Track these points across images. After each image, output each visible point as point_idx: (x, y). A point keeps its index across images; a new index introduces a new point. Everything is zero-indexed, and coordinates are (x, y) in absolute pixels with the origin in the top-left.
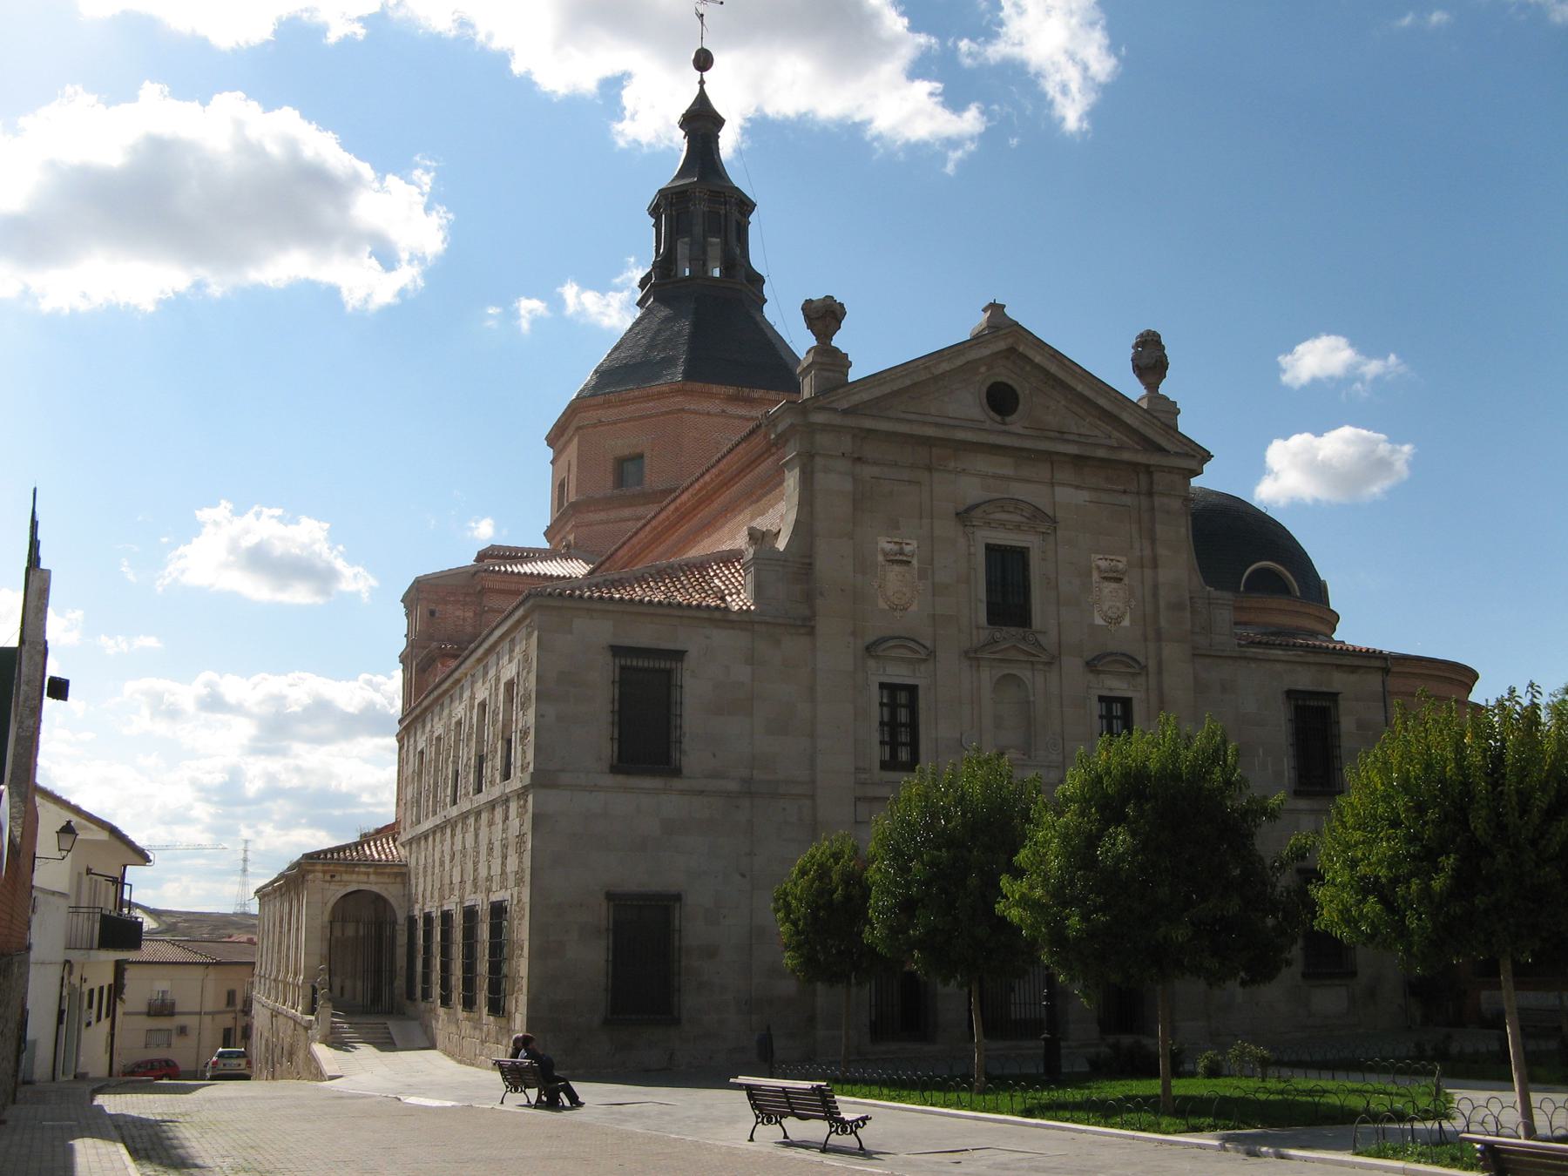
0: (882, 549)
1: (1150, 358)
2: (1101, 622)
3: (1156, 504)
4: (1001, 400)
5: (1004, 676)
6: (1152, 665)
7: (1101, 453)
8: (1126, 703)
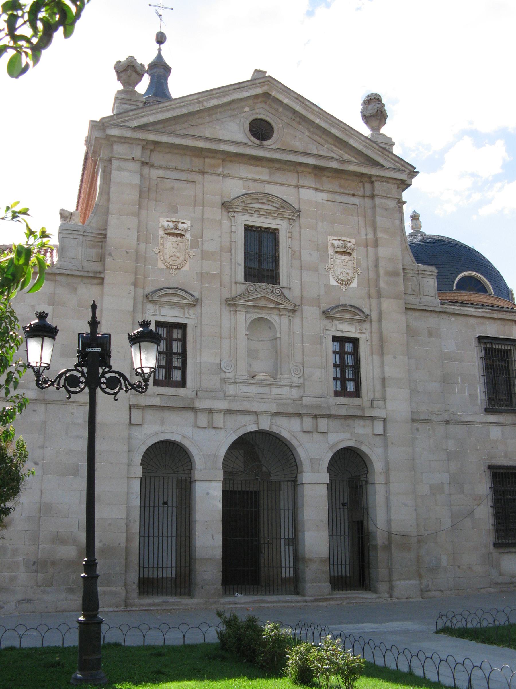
0: (163, 226)
1: (375, 111)
2: (336, 284)
3: (377, 203)
4: (261, 130)
5: (259, 319)
6: (374, 316)
7: (334, 165)
8: (355, 341)
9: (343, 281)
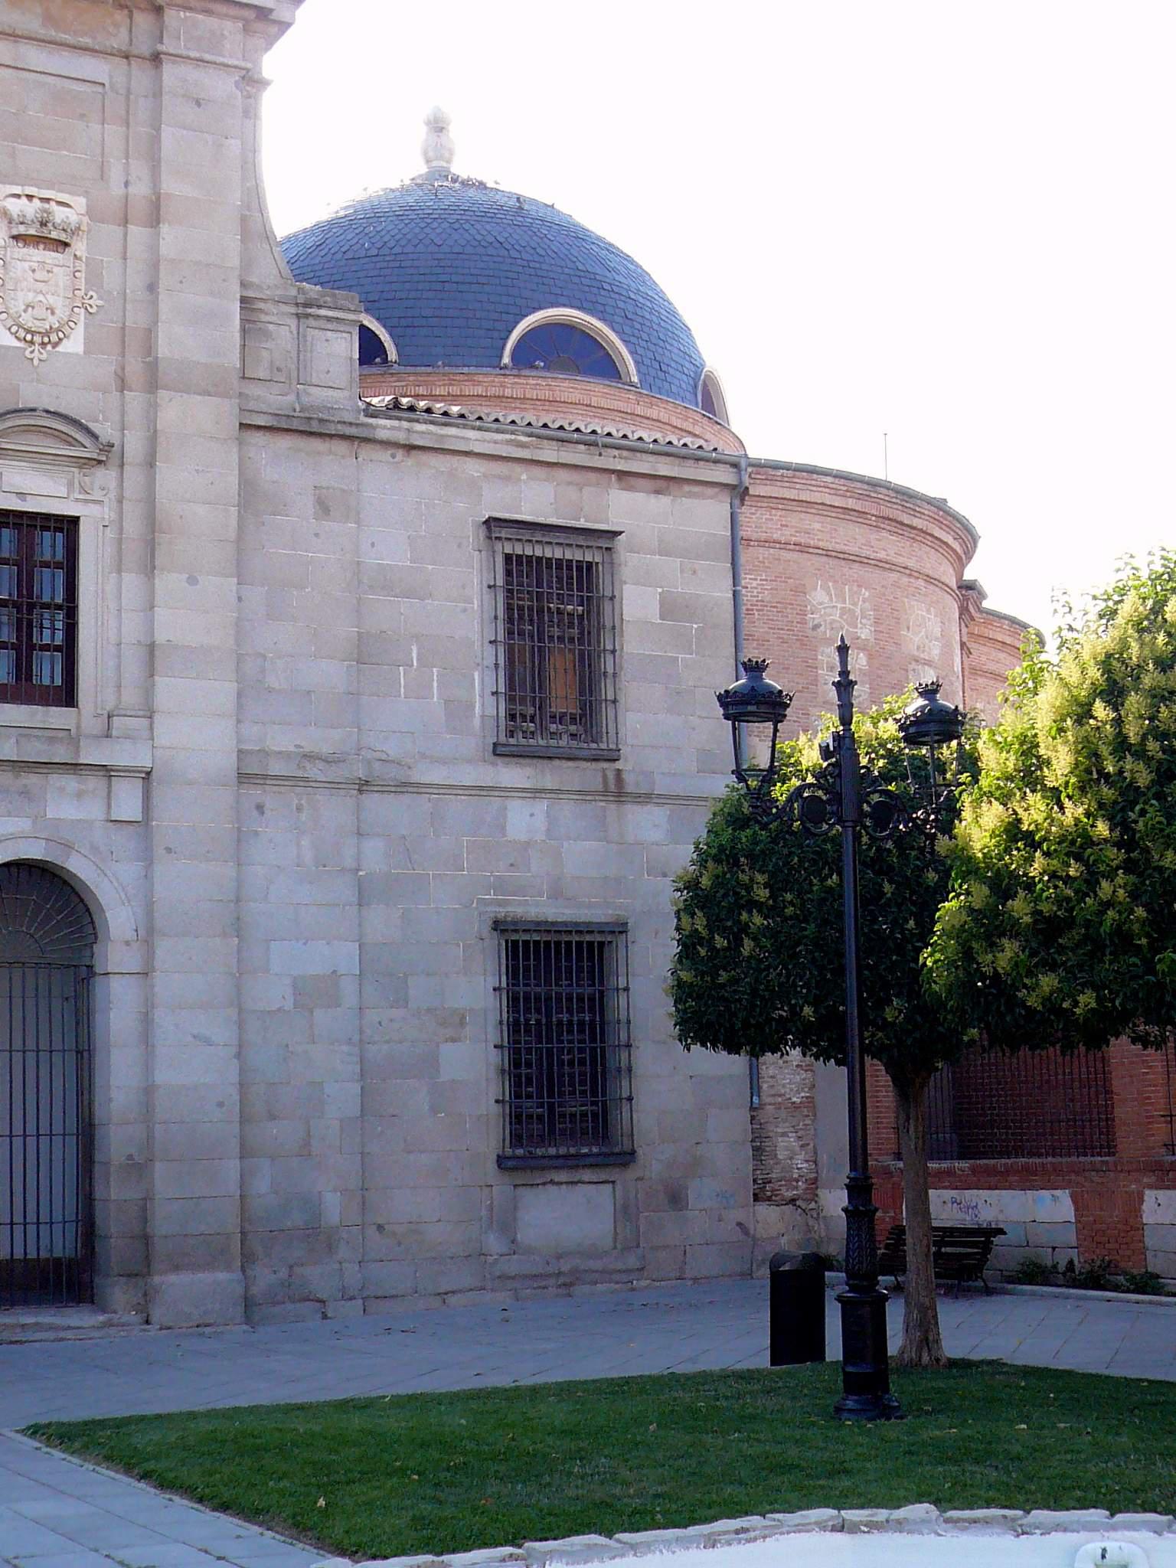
6: (134, 446)
9: (33, 333)
